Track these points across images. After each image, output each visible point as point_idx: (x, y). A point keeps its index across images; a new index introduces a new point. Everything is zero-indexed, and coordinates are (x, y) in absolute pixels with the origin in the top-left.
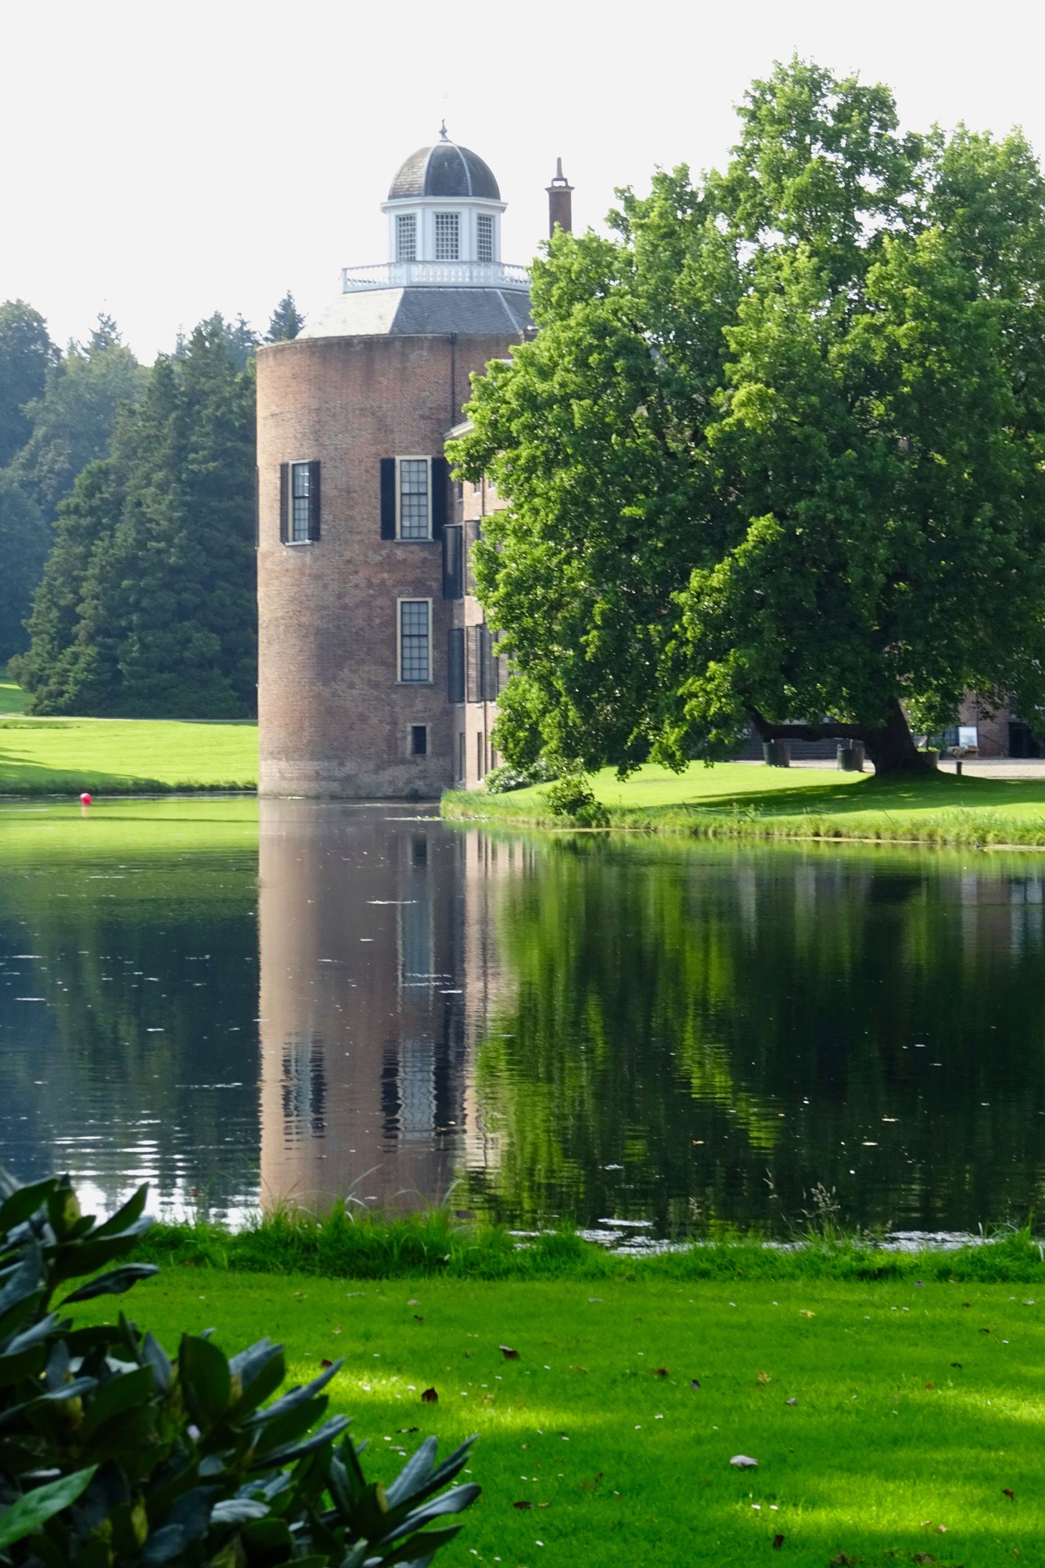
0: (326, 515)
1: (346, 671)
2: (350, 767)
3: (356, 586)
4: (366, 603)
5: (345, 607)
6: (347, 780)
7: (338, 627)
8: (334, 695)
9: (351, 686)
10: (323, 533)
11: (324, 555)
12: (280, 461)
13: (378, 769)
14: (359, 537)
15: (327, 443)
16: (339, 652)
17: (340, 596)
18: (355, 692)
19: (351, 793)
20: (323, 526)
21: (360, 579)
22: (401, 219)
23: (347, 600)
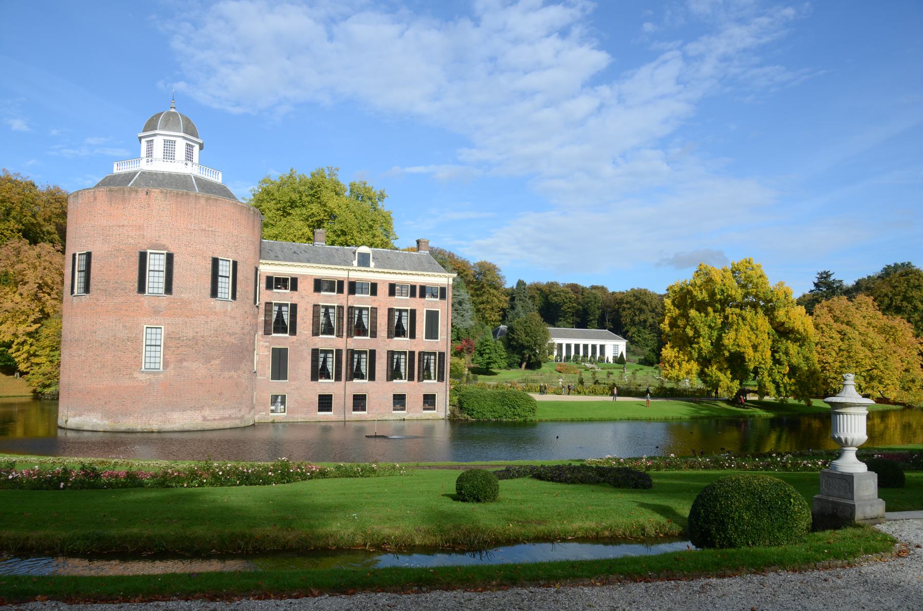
0: (238, 288)
1: (243, 365)
2: (242, 413)
3: (247, 324)
4: (249, 333)
5: (244, 334)
6: (242, 417)
7: (241, 343)
8: (239, 376)
9: (244, 373)
10: (237, 296)
11: (237, 308)
12: (210, 255)
13: (250, 411)
14: (249, 301)
15: (240, 253)
16: (241, 356)
17: (242, 329)
18: (245, 375)
19: (243, 425)
20: (238, 293)
21: (248, 321)
22: (187, 145)
23: (245, 331)
